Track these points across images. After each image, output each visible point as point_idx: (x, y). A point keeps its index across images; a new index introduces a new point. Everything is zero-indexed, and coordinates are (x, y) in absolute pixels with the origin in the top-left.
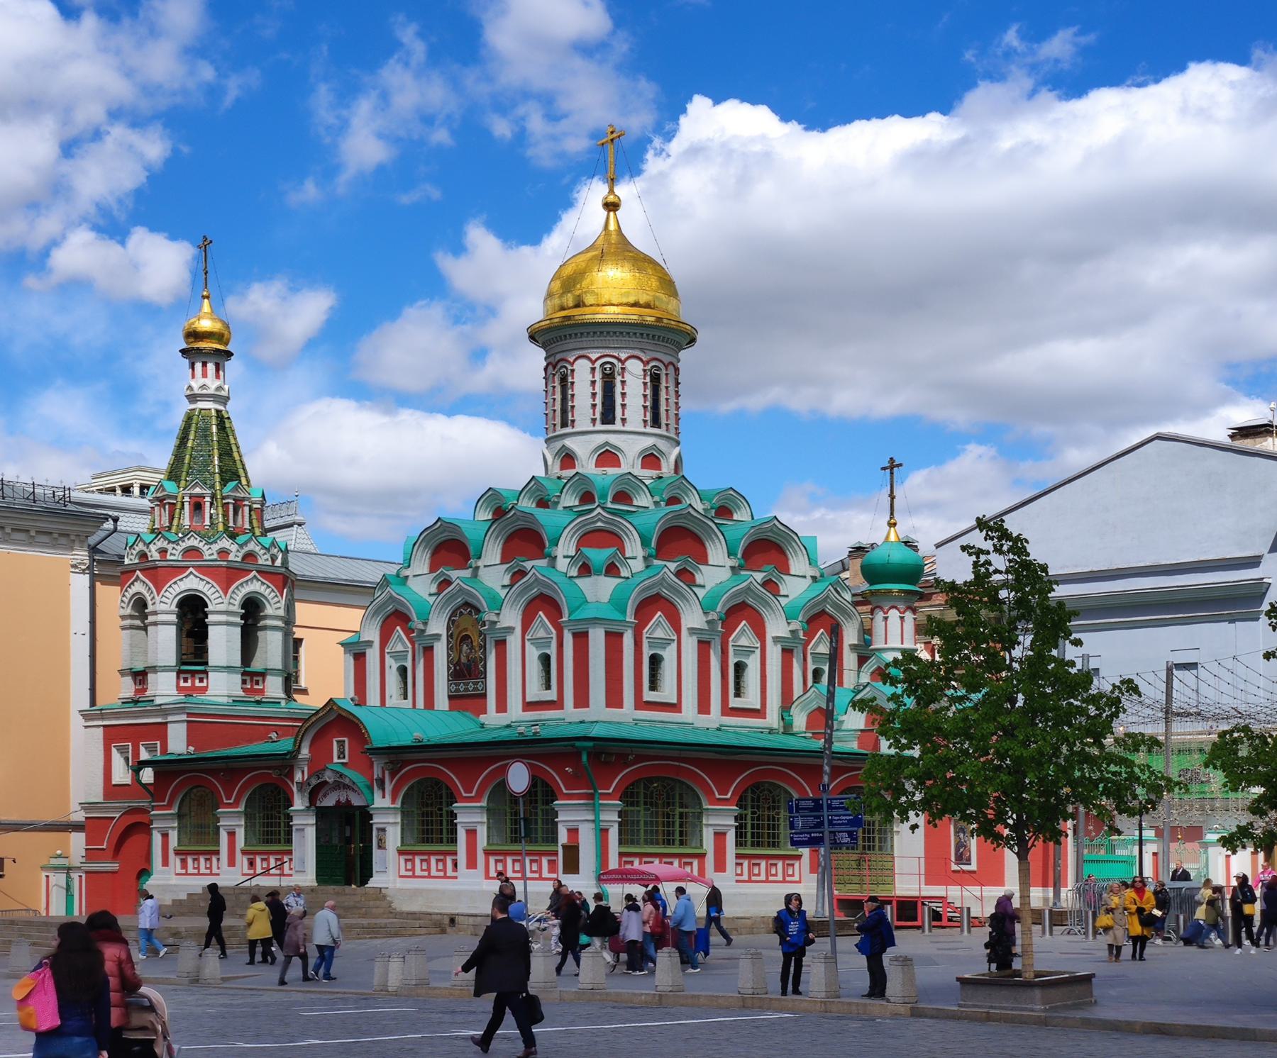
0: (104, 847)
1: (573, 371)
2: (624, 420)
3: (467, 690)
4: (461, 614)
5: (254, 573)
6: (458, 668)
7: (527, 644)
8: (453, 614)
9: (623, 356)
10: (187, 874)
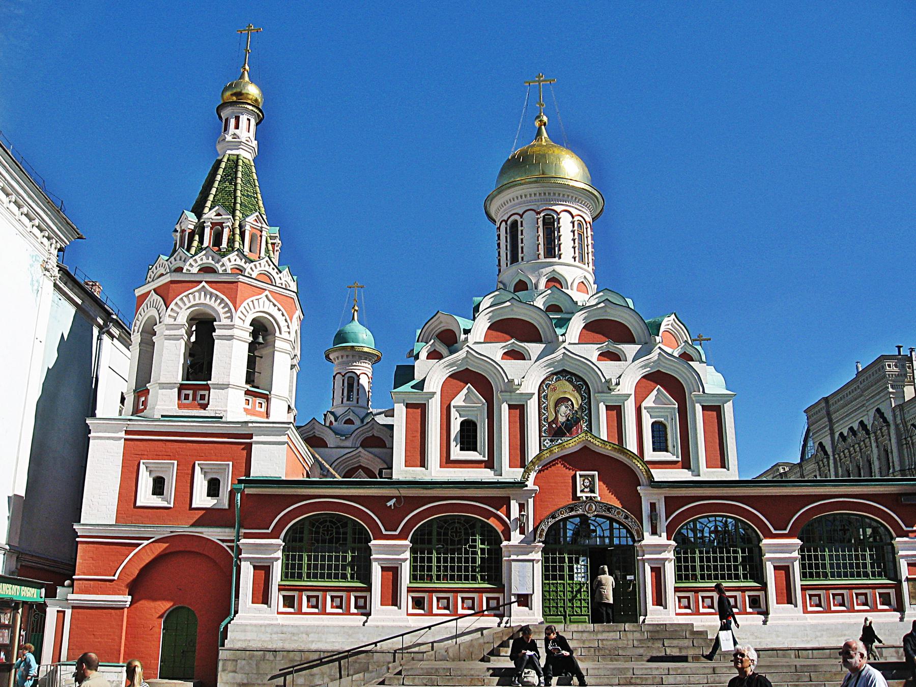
0: (116, 578)
1: (559, 219)
2: (588, 264)
6: (554, 426)
7: (644, 412)
10: (300, 612)
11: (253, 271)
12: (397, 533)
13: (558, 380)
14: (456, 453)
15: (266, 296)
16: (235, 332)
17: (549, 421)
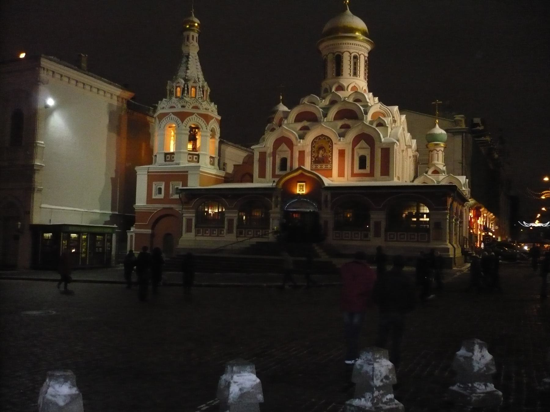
0: (147, 224)
3: (322, 168)
4: (320, 139)
5: (215, 118)
6: (317, 159)
8: (316, 138)
9: (360, 53)
11: (189, 106)
12: (233, 207)
13: (320, 139)
14: (278, 172)
15: (196, 115)
16: (183, 132)
17: (315, 157)
